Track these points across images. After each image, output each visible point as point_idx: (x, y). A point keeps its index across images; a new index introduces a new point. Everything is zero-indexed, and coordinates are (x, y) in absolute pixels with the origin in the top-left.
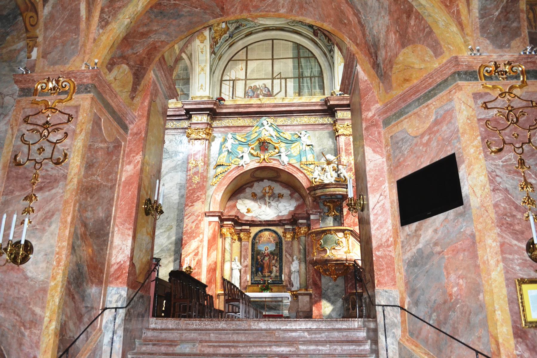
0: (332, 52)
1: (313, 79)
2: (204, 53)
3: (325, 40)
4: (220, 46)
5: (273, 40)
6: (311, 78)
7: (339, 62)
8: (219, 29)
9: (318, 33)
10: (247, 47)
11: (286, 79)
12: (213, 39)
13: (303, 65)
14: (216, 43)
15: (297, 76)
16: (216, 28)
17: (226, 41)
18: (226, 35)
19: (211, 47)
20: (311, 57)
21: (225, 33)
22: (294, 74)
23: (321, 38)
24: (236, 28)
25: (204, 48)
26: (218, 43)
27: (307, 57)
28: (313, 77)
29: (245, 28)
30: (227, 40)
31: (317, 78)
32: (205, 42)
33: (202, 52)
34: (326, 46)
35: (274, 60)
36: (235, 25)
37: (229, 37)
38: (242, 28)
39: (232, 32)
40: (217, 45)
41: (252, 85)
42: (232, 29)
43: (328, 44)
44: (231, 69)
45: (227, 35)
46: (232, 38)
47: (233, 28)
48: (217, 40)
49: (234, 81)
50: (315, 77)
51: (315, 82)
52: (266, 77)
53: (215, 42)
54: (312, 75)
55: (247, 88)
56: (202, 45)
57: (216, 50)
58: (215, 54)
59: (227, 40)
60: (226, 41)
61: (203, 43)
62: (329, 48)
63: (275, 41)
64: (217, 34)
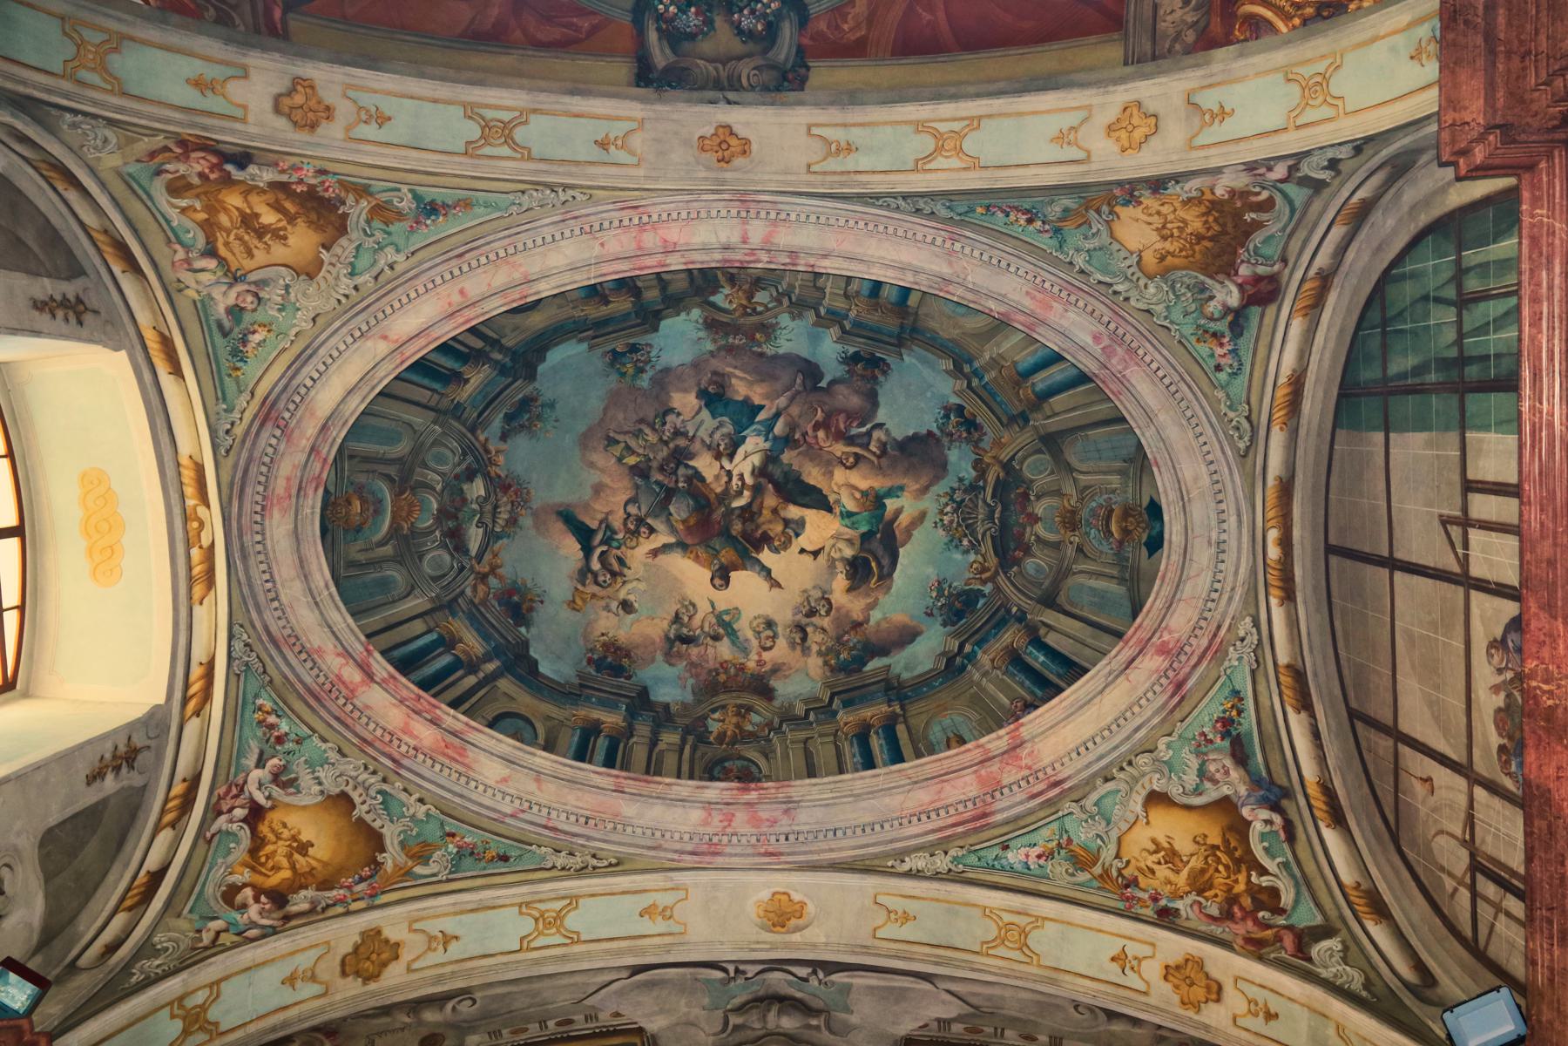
0: (1306, 169)
1: (1473, 284)
2: (1275, 1004)
3: (1273, 228)
4: (1304, 883)
5: (1330, 550)
6: (1464, 302)
7: (1326, 112)
8: (1196, 863)
9: (1258, 279)
10: (1353, 715)
11: (1470, 487)
12: (1227, 916)
13: (1411, 361)
14: (1268, 899)
15: (1454, 400)
16: (1182, 879)
17: (1291, 838)
18: (1258, 827)
19: (1256, 948)
20: (1383, 309)
21: (1240, 828)
22: (1447, 429)
23: (1273, 250)
24: (1240, 755)
25: (1253, 991)
26: (1274, 893)
27: (1384, 334)
28: (1459, 287)
29: (1250, 704)
30: (1289, 827)
31: (1471, 256)
32: (1215, 973)
33: (1270, 1016)
34: (1298, 217)
35: (1399, 555)
36: (1220, 761)
37: (1276, 807)
38: (1249, 721)
39: (1256, 782)
40: (1287, 898)
41: (1495, 740)
42: (1234, 783)
43: (1278, 198)
44: (1429, 853)
45: (1259, 819)
46: (1287, 793)
47: (1235, 774)
48: (1252, 890)
49: (1476, 867)
50: (1460, 272)
51: (1484, 266)
52: (1460, 629)
53: (1259, 905)
54: (1450, 293)
55: (1509, 784)
56: (1234, 1001)
57: (1306, 916)
58: (1326, 932)
59: (1289, 827)
60: (1291, 838)
61: (1220, 988)
62: (1298, 194)
63: (1333, 540)
64: (1220, 880)
